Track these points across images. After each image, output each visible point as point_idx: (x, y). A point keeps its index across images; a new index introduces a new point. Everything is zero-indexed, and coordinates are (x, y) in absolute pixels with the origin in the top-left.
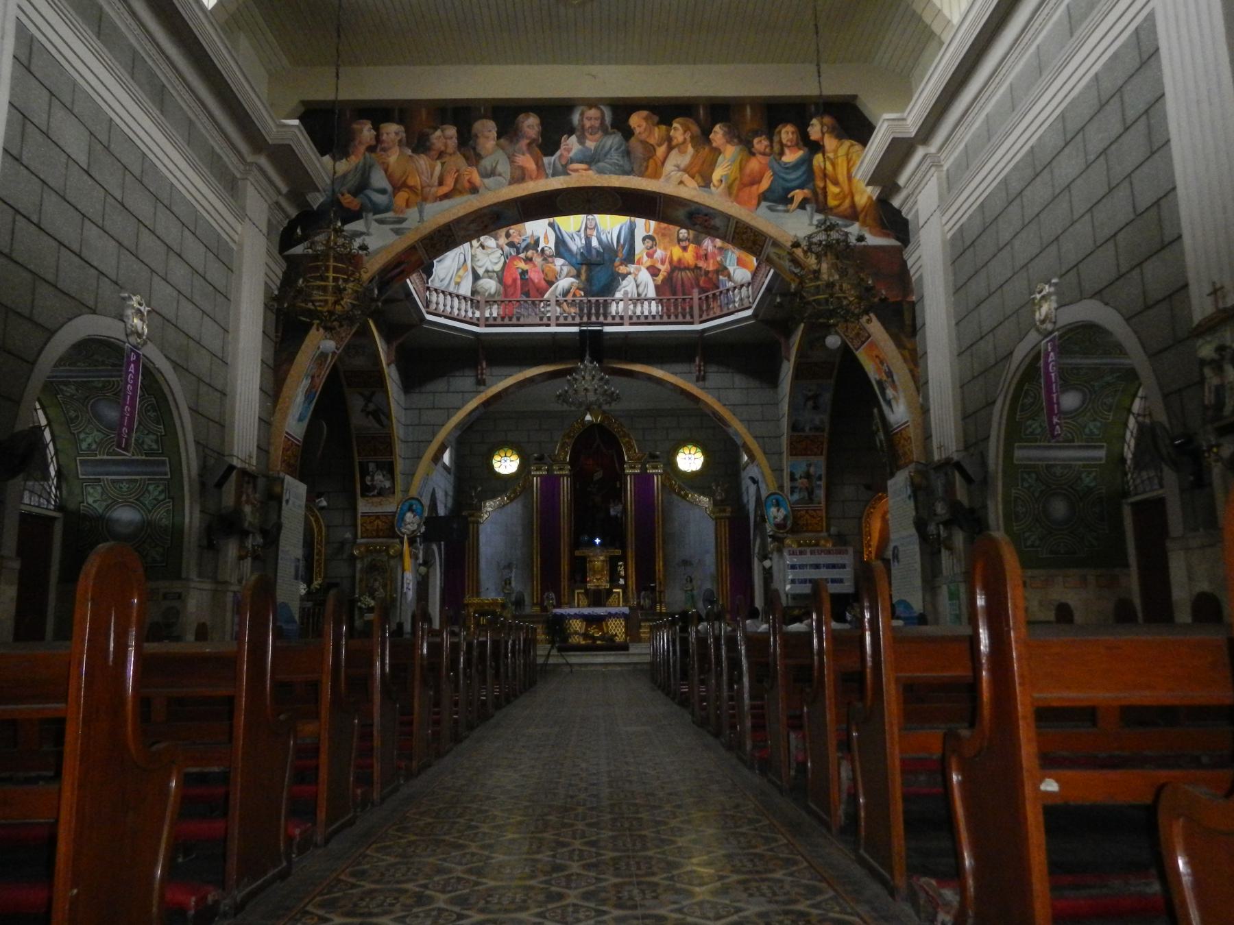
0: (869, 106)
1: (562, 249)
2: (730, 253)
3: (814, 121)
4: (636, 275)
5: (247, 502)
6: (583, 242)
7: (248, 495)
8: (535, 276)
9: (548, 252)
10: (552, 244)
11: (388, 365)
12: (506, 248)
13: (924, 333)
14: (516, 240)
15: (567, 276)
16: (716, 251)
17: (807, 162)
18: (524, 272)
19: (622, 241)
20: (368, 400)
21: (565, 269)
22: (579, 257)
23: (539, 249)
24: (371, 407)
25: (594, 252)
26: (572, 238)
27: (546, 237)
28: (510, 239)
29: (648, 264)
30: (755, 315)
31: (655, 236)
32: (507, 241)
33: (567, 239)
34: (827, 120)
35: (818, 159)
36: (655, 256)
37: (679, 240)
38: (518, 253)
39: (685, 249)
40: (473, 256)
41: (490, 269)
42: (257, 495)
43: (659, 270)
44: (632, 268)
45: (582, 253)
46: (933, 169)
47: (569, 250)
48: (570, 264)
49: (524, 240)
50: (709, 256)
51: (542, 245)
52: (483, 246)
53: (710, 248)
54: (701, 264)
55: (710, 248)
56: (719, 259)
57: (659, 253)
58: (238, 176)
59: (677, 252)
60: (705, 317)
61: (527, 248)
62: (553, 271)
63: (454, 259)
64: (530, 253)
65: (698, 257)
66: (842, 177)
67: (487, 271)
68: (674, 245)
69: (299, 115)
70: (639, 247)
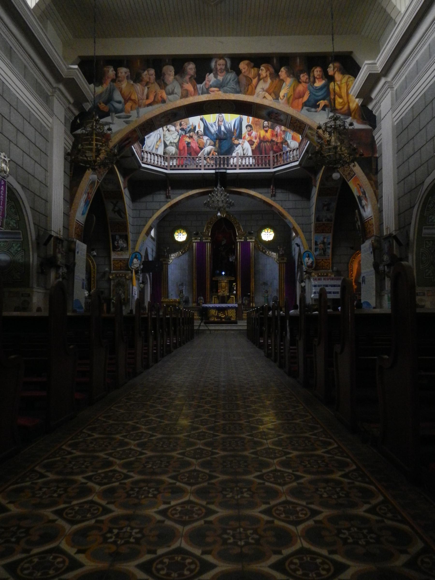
0: (358, 57)
1: (207, 132)
2: (288, 133)
3: (331, 65)
4: (243, 145)
5: (59, 252)
6: (217, 128)
7: (59, 249)
8: (194, 145)
9: (200, 133)
10: (202, 129)
11: (124, 188)
12: (180, 131)
13: (382, 174)
14: (185, 127)
15: (209, 145)
16: (282, 133)
17: (326, 86)
18: (189, 143)
19: (236, 128)
20: (115, 205)
21: (209, 142)
22: (215, 136)
23: (196, 132)
24: (117, 208)
25: (222, 133)
26: (212, 126)
27: (199, 125)
28: (182, 127)
29: (249, 139)
30: (300, 164)
31: (252, 125)
32: (180, 128)
33: (210, 127)
34: (337, 64)
35: (332, 85)
36: (252, 135)
37: (264, 127)
38: (186, 133)
39: (266, 131)
40: (164, 135)
41: (172, 141)
42: (64, 249)
43: (254, 142)
44: (241, 141)
45: (216, 134)
46: (389, 89)
47: (210, 132)
48: (211, 139)
49: (188, 127)
50: (278, 135)
51: (197, 129)
52: (168, 130)
53: (279, 131)
54: (274, 139)
55: (279, 131)
56: (283, 136)
57: (254, 134)
58: (49, 94)
59: (262, 133)
60: (276, 165)
61: (190, 131)
62: (203, 143)
63: (155, 136)
64: (191, 134)
65: (273, 135)
66: (344, 94)
67: (171, 143)
68: (261, 130)
69: (78, 63)
70: (244, 131)
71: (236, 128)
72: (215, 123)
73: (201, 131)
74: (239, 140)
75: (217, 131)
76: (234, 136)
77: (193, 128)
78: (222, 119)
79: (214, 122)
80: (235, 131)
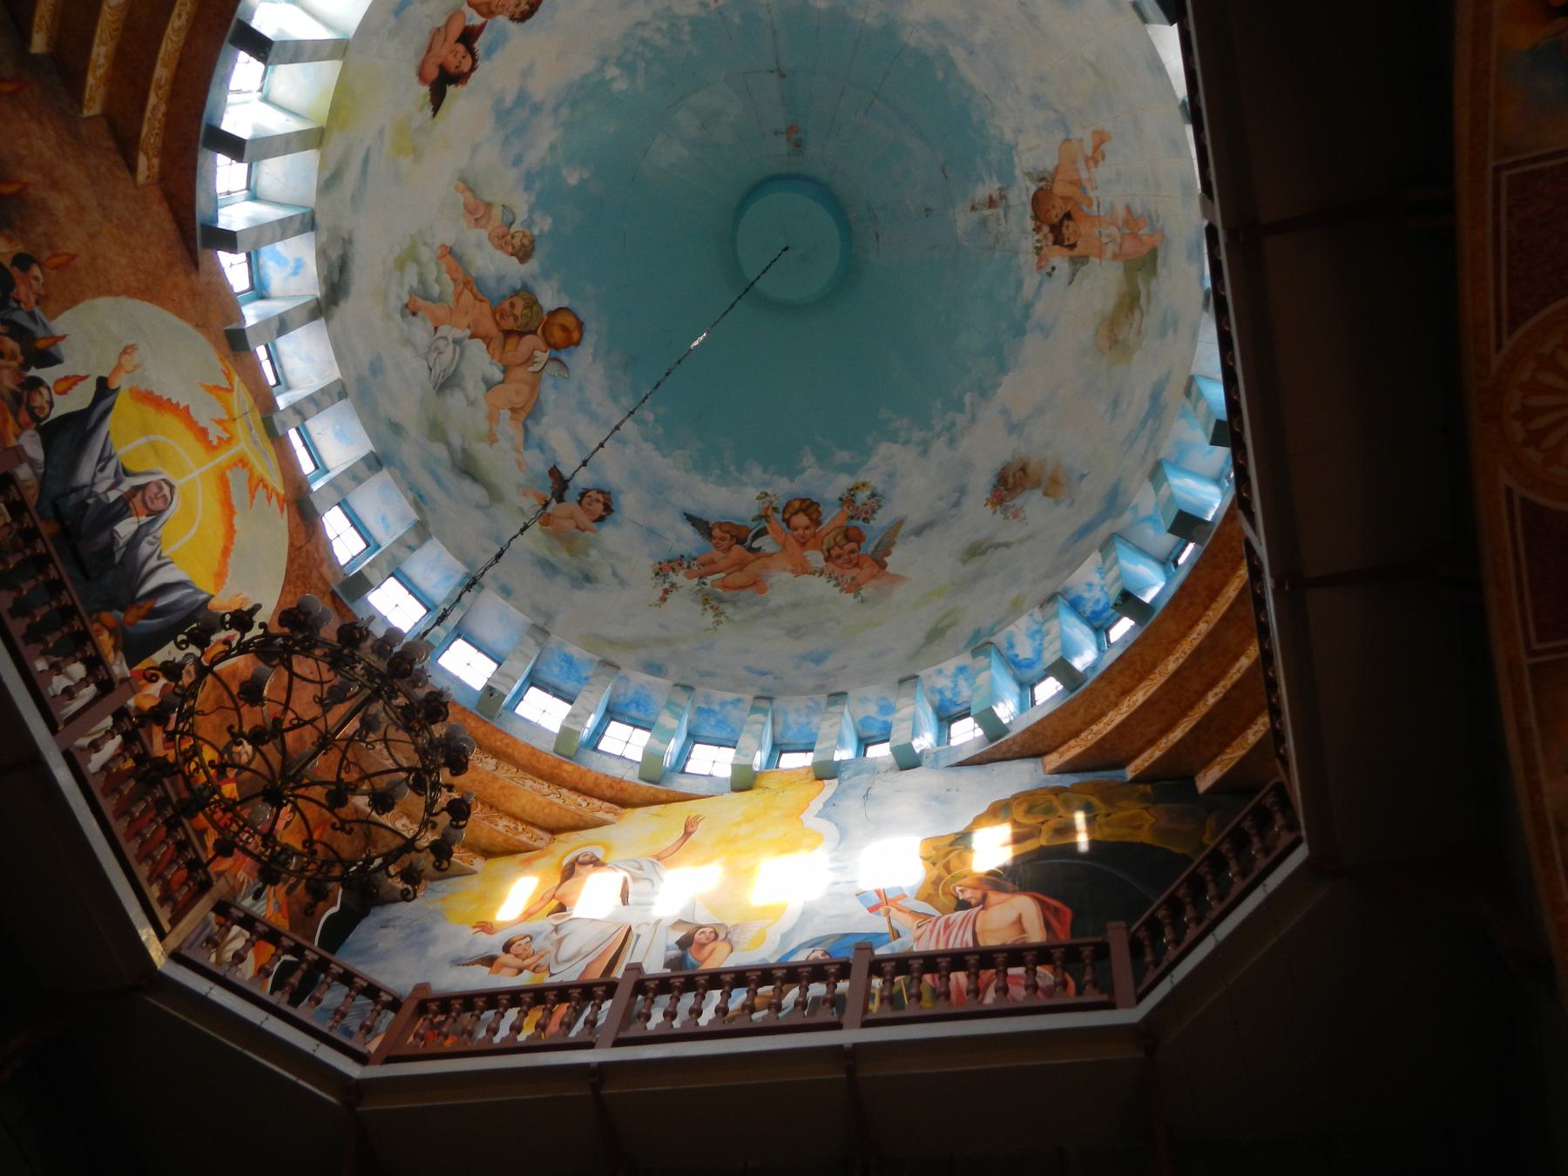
6: (113, 496)
9: (39, 400)
19: (162, 602)
22: (73, 498)
23: (33, 372)
25: (103, 538)
26: (104, 459)
27: (72, 381)
28: (15, 271)
45: (83, 505)
47: (73, 466)
49: (32, 315)
51: (49, 375)
71: (162, 602)
72: (127, 473)
73: (51, 405)
74: (120, 654)
75: (99, 501)
76: (121, 615)
77: (41, 344)
78: (159, 505)
79: (130, 466)
80: (148, 605)
